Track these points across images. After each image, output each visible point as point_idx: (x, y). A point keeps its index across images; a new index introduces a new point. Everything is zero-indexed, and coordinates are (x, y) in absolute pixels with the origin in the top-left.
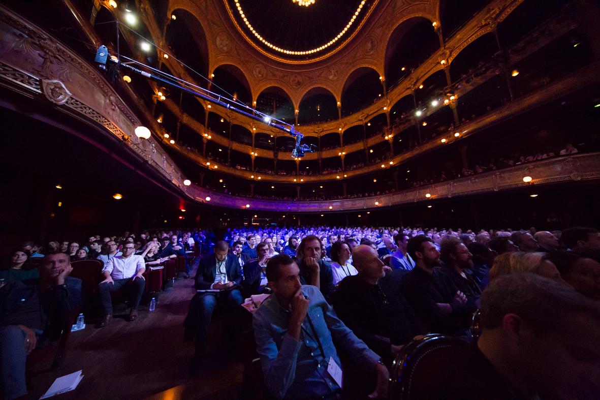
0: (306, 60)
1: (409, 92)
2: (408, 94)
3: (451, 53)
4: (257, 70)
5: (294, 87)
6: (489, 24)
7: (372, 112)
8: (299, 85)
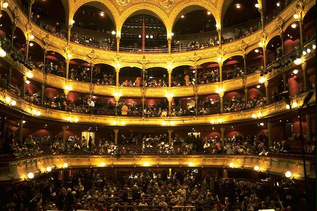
5: (166, 7)
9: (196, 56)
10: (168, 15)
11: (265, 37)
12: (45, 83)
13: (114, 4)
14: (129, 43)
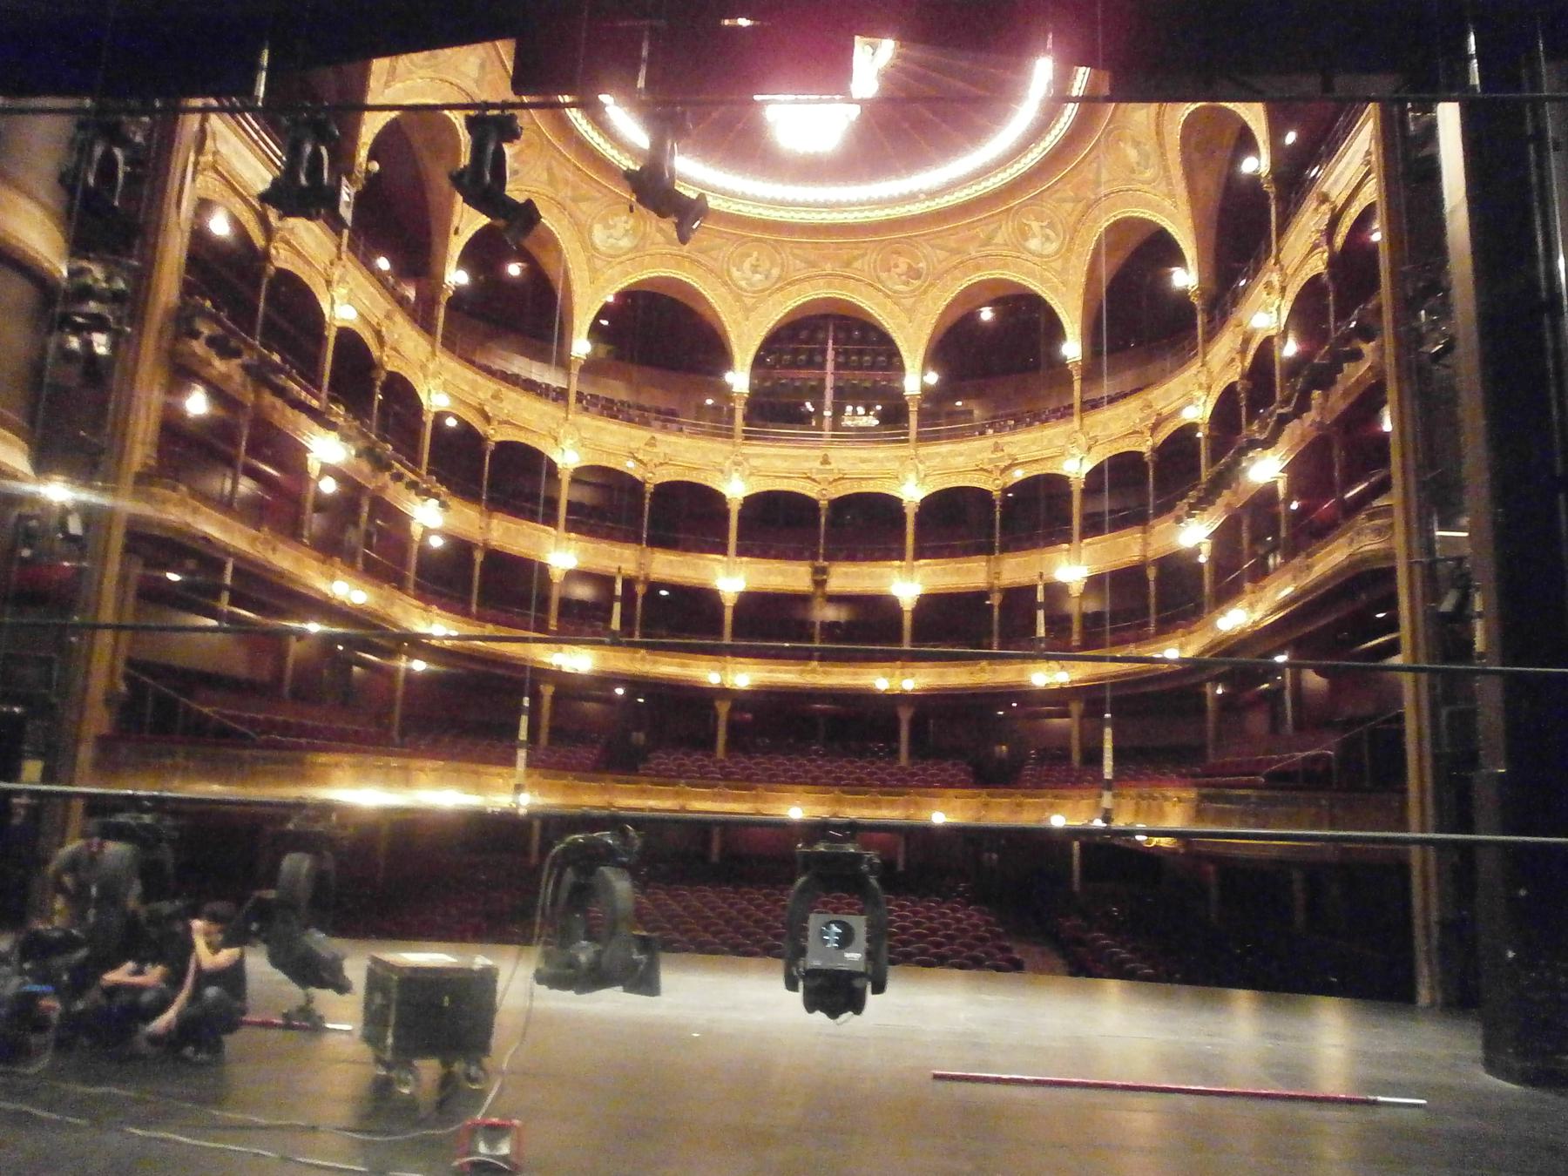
8: (918, 277)
9: (1000, 454)
10: (910, 311)
12: (486, 544)
13: (725, 284)
14: (776, 411)
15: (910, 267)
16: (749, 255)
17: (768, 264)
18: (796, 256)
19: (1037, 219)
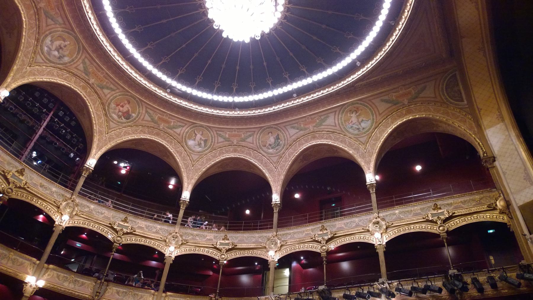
0: (166, 92)
1: (316, 248)
2: (314, 250)
3: (387, 228)
4: (57, 43)
5: (115, 116)
6: (436, 223)
7: (244, 246)
8: (127, 119)
11: (279, 245)
13: (38, 40)
15: (128, 112)
16: (64, 40)
17: (67, 53)
18: (84, 63)
19: (202, 135)
